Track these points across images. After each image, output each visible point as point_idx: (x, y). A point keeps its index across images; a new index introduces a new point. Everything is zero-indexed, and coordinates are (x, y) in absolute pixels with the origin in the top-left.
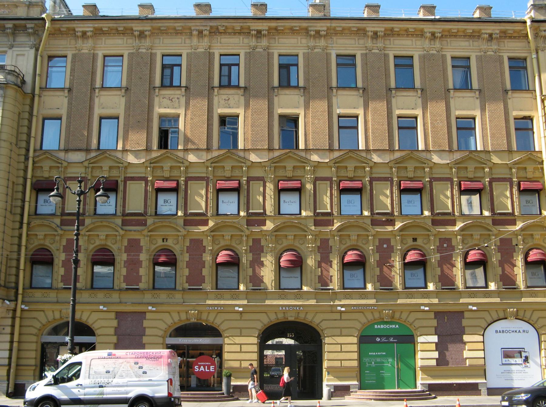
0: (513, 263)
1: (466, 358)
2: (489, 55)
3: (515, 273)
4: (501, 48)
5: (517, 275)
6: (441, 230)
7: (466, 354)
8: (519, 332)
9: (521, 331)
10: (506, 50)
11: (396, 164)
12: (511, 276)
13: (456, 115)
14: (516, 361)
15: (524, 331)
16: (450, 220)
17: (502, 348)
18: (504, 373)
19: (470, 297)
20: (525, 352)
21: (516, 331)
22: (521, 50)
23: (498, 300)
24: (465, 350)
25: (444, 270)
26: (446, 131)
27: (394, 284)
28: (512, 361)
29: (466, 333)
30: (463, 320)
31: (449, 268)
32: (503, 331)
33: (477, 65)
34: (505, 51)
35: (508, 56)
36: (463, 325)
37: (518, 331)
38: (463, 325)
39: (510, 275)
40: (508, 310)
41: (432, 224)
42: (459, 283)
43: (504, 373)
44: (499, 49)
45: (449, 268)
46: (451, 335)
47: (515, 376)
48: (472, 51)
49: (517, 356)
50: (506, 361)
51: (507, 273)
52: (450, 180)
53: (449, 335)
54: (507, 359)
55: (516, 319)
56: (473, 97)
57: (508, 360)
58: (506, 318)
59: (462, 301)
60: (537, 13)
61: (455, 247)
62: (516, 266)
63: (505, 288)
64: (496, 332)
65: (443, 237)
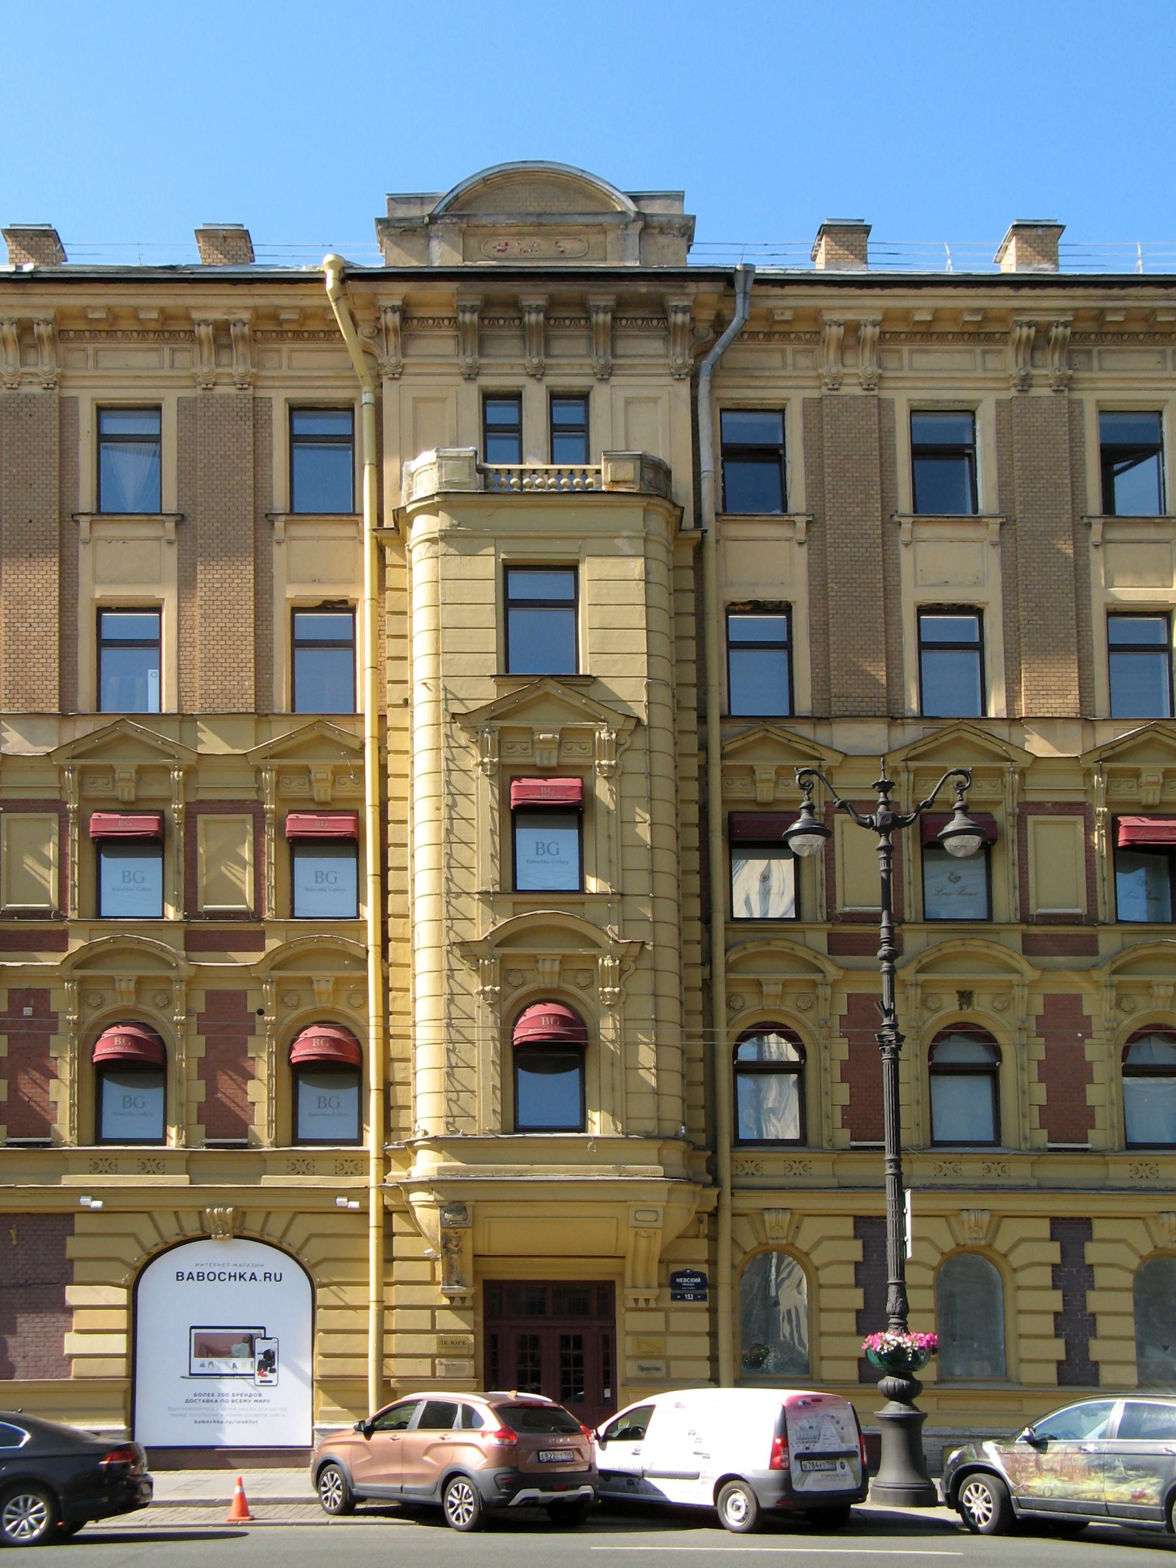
0: (244, 1068)
1: (71, 1357)
2: (221, 396)
3: (250, 1099)
4: (264, 373)
5: (253, 1104)
6: (8, 964)
7: (73, 1343)
8: (253, 1277)
9: (260, 1276)
10: (285, 378)
11: (74, 758)
12: (237, 1109)
13: (93, 599)
14: (234, 1366)
15: (267, 1276)
16: (49, 932)
17: (192, 1327)
18: (191, 1401)
19: (96, 1169)
20: (265, 1338)
21: (241, 1276)
22: (335, 378)
23: (182, 1180)
24: (70, 1331)
25: (21, 1086)
26: (54, 651)
27: (55, 1130)
28: (222, 1365)
29: (76, 1278)
30: (70, 1240)
31: (34, 1081)
32: (201, 1276)
33: (180, 430)
34: (277, 384)
35: (287, 400)
36: (68, 1255)
37: (247, 1276)
38: (68, 1255)
39: (232, 1105)
40: (208, 1210)
41: (187, 948)
42: (64, 1126)
43: (191, 1401)
44: (258, 377)
45: (34, 1081)
46: (26, 1285)
47: (228, 1411)
48: (167, 383)
49: (239, 1351)
50: (202, 1365)
51: (225, 1099)
52: (56, 806)
53: (21, 1286)
54: (206, 1360)
55: (236, 1237)
56: (158, 539)
57: (211, 1363)
58: (209, 1238)
59: (68, 1181)
60: (397, 251)
61: (60, 1016)
62: (253, 1078)
63: (209, 1145)
64: (179, 1276)
65: (25, 986)
